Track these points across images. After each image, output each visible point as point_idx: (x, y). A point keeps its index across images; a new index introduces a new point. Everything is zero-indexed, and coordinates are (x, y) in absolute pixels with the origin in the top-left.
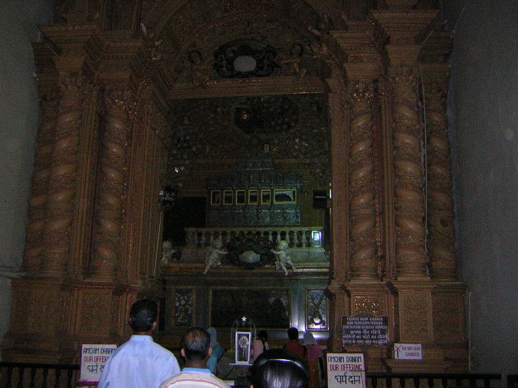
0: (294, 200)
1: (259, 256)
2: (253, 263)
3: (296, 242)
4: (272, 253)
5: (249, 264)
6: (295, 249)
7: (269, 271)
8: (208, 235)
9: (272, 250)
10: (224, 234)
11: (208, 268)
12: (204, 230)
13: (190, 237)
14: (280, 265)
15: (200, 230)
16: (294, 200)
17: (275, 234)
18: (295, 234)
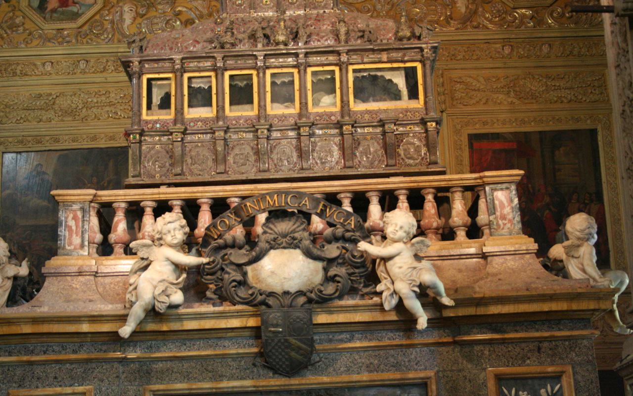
0: (414, 94)
1: (319, 265)
2: (300, 293)
3: (435, 222)
4: (363, 254)
5: (286, 293)
6: (434, 246)
7: (359, 317)
8: (135, 212)
9: (363, 246)
10: (191, 210)
11: (137, 312)
12: (120, 197)
13: (72, 223)
14: (395, 292)
15: (106, 195)
16: (414, 94)
17: (360, 203)
18: (430, 197)
